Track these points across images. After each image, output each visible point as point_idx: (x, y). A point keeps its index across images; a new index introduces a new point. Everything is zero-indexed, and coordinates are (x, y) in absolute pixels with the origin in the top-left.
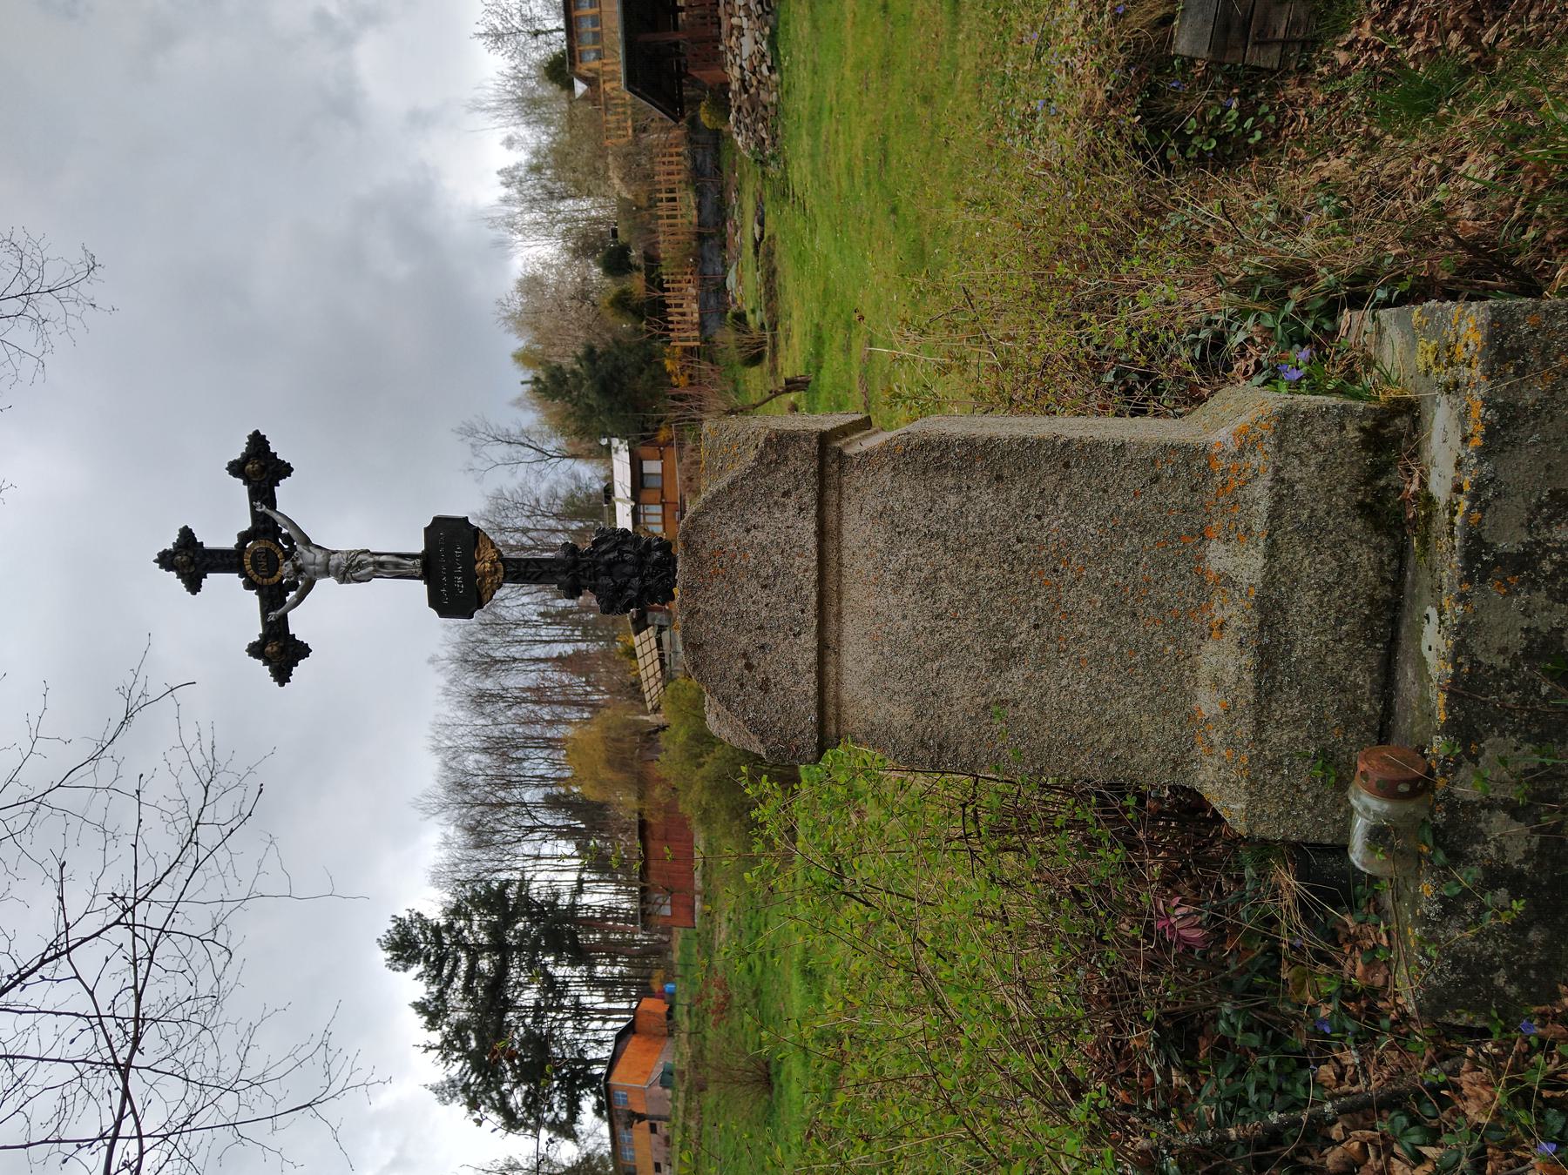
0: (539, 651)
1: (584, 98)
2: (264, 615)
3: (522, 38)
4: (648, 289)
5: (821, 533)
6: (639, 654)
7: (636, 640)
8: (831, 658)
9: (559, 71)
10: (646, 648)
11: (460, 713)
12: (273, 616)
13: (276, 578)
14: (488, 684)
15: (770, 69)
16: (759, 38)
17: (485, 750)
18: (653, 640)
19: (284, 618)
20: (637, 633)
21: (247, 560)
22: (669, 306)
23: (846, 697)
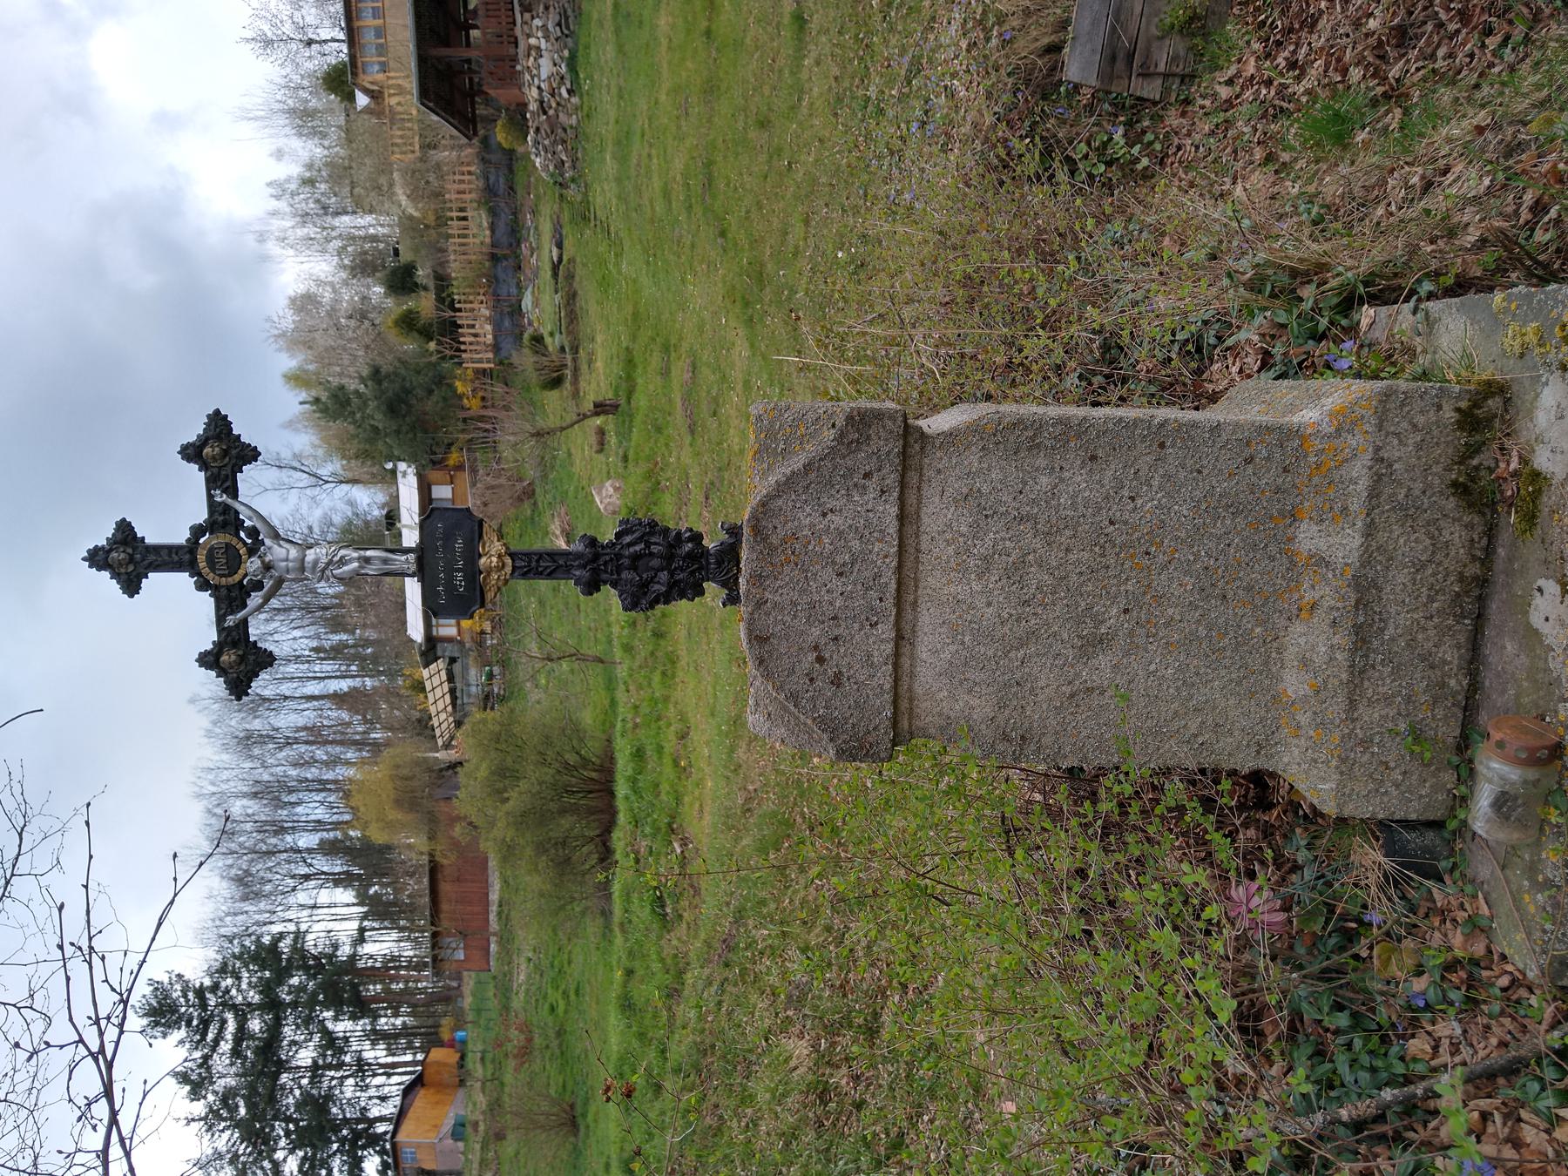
0: (313, 688)
1: (366, 110)
2: (220, 619)
3: (293, 46)
4: (438, 309)
5: (902, 518)
6: (428, 688)
7: (426, 673)
8: (906, 650)
9: (339, 81)
10: (436, 681)
11: (225, 757)
12: (231, 621)
13: (237, 578)
14: (257, 725)
15: (569, 92)
16: (558, 60)
17: (255, 795)
18: (443, 673)
19: (244, 623)
20: (426, 665)
21: (201, 557)
22: (460, 326)
23: (919, 690)
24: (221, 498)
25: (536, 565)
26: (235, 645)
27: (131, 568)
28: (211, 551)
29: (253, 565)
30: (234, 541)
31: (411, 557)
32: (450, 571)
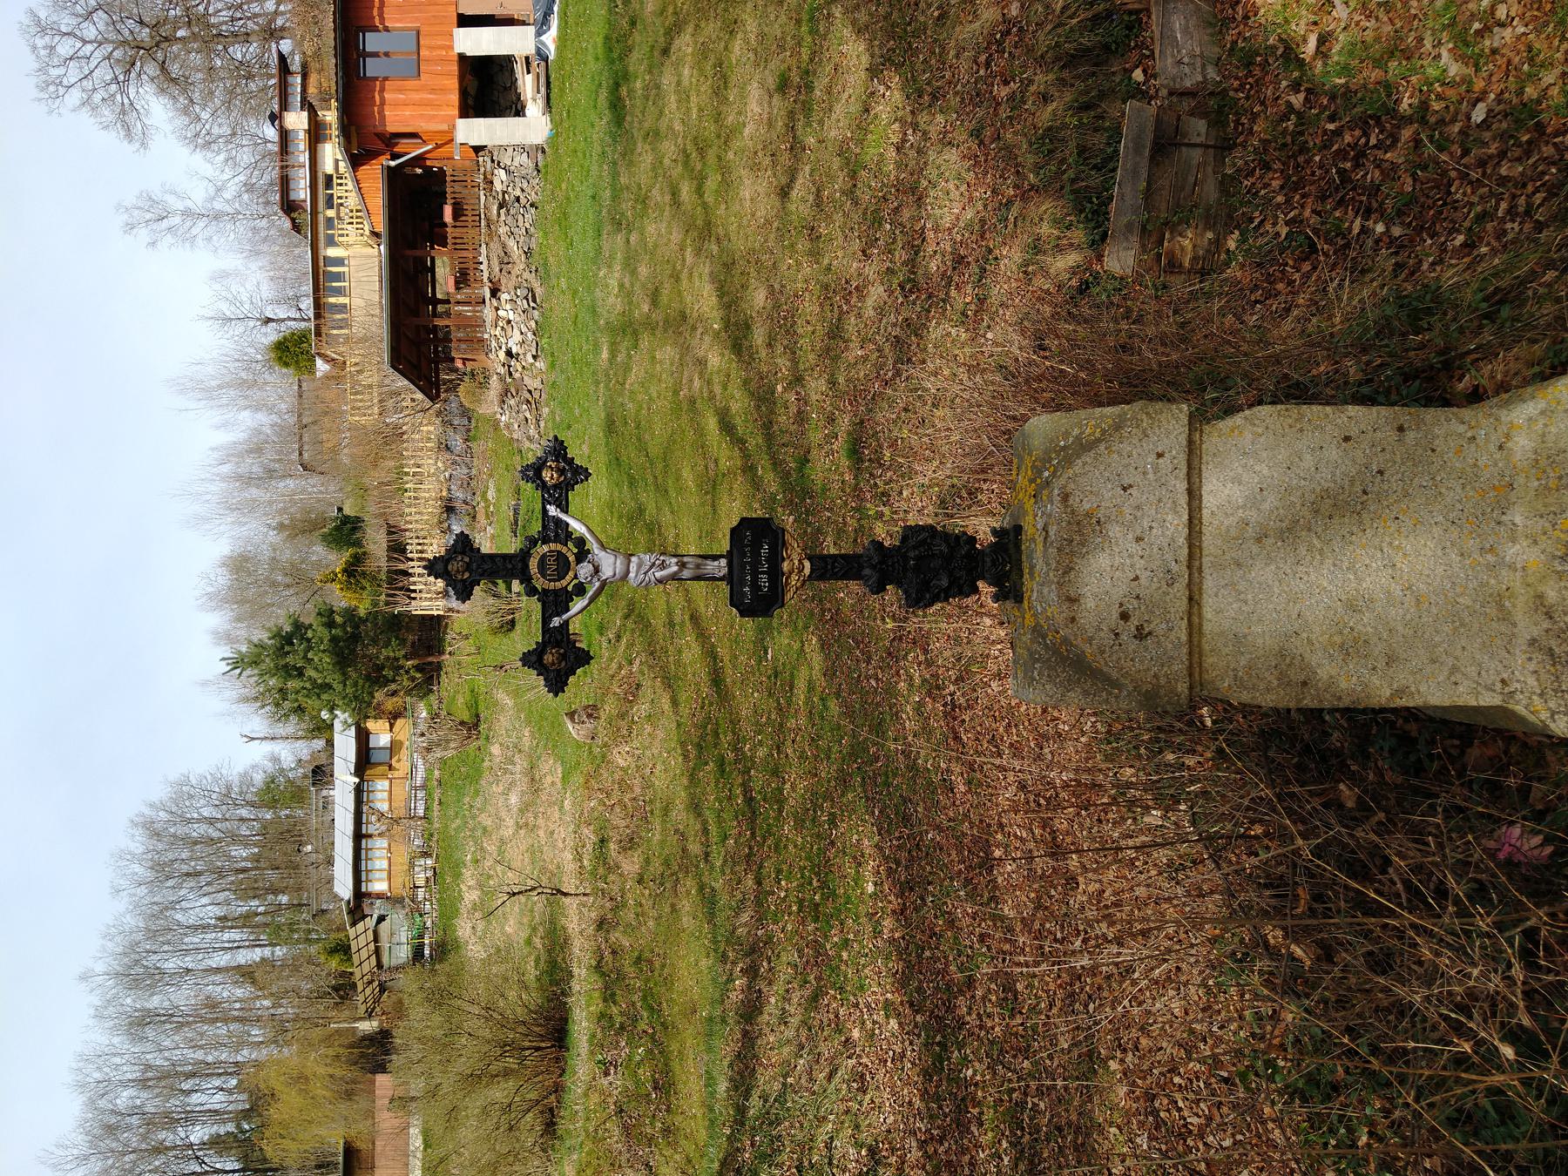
0: (221, 960)
1: (327, 377)
2: (546, 620)
3: (251, 324)
4: (390, 559)
5: (1190, 492)
6: (354, 949)
7: (352, 932)
8: (1195, 610)
9: (291, 352)
10: (362, 941)
11: (116, 1040)
12: (556, 622)
13: (564, 583)
14: (155, 1002)
15: (534, 357)
16: (524, 330)
17: (143, 1083)
18: (370, 933)
19: (567, 622)
20: (353, 924)
21: (533, 564)
22: (411, 575)
23: (1206, 647)
24: (553, 510)
25: (827, 568)
26: (558, 645)
27: (467, 575)
28: (543, 557)
29: (584, 570)
30: (564, 550)
31: (723, 562)
32: (755, 574)
